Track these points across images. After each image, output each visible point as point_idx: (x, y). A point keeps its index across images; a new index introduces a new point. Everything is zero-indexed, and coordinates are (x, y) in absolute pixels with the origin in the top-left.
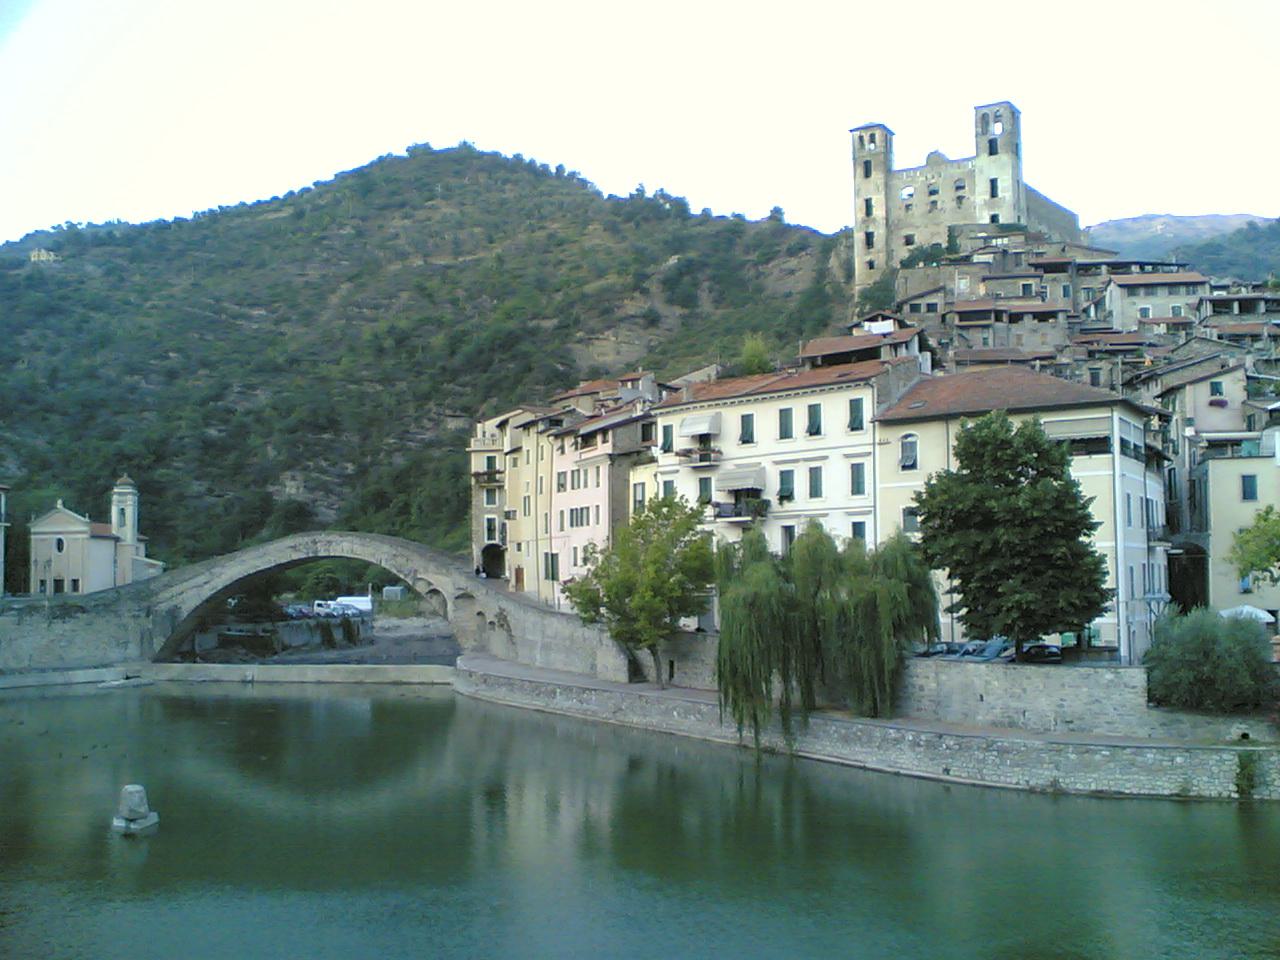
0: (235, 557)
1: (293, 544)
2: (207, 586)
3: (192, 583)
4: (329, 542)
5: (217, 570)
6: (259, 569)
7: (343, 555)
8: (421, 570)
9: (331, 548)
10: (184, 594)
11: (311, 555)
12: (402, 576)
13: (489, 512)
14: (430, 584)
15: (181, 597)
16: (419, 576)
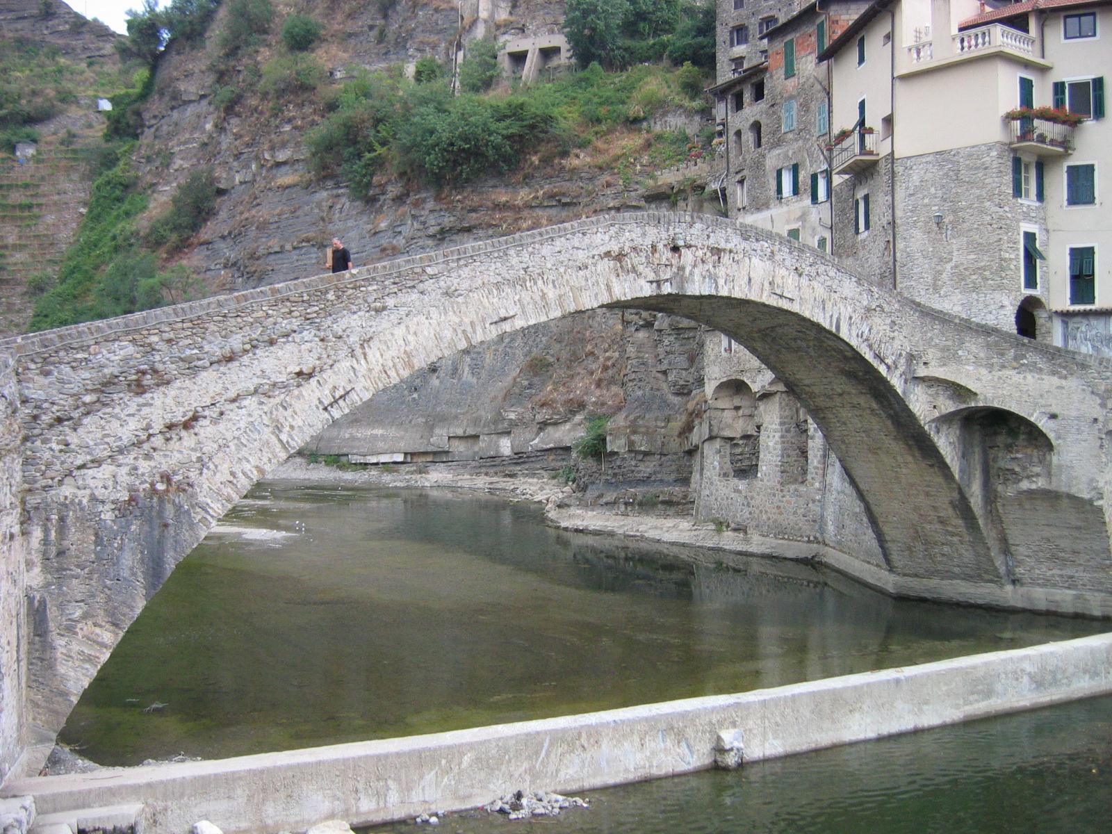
0: (420, 276)
1: (615, 247)
2: (312, 392)
3: (241, 377)
4: (717, 252)
5: (353, 323)
6: (507, 327)
7: (753, 296)
8: (932, 355)
9: (721, 272)
10: (205, 429)
11: (667, 289)
12: (882, 370)
13: (1027, 217)
14: (959, 391)
15: (188, 439)
16: (922, 372)
